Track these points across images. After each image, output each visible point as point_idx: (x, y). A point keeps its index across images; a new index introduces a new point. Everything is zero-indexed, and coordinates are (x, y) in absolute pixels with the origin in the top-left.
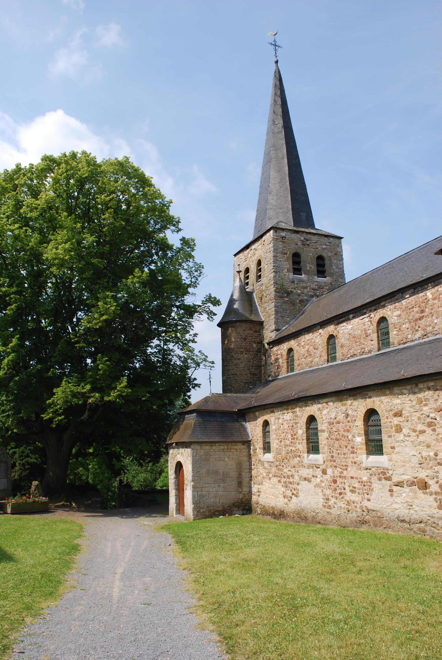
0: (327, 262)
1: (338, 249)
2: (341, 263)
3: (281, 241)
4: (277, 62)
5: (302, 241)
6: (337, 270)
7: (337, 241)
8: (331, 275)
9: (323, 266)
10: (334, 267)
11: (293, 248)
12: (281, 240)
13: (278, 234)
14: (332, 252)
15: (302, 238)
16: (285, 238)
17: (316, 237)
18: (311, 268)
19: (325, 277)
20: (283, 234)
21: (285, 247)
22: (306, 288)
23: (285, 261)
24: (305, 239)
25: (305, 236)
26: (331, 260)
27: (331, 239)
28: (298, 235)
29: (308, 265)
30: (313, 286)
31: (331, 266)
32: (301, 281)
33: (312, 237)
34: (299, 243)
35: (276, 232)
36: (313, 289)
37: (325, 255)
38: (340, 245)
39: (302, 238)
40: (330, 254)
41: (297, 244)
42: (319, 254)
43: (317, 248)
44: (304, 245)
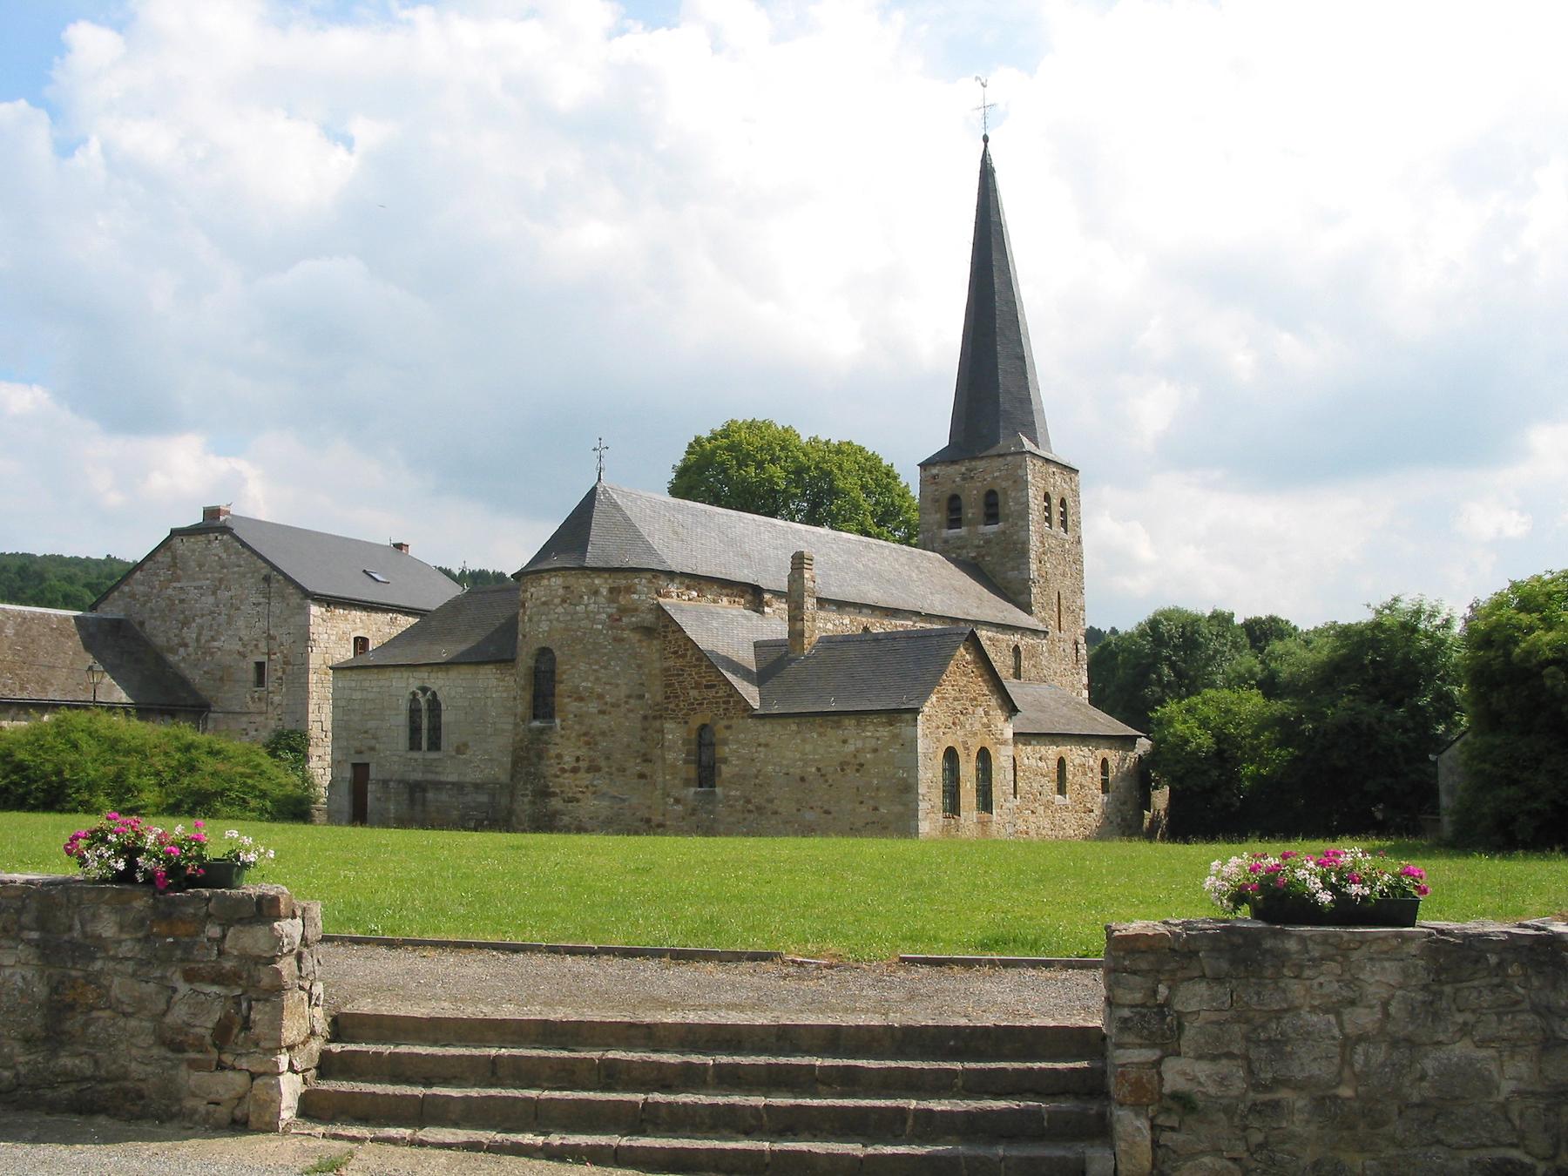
0: (1001, 498)
1: (1020, 472)
2: (1024, 493)
3: (932, 484)
4: (986, 139)
5: (963, 474)
6: (1017, 507)
7: (1019, 457)
8: (1006, 521)
9: (997, 505)
10: (1011, 504)
11: (948, 489)
12: (933, 481)
13: (928, 473)
14: (1008, 479)
15: (963, 469)
16: (938, 475)
17: (984, 462)
18: (973, 514)
19: (997, 524)
20: (935, 471)
21: (936, 490)
22: (963, 547)
23: (936, 512)
24: (967, 470)
25: (968, 464)
26: (1006, 493)
27: (1009, 458)
28: (957, 467)
29: (970, 511)
30: (976, 542)
31: (1006, 503)
32: (959, 538)
33: (978, 463)
34: (958, 479)
35: (925, 470)
36: (978, 547)
37: (997, 489)
38: (1024, 464)
39: (963, 469)
40: (1004, 484)
41: (954, 482)
42: (988, 489)
43: (985, 480)
44: (964, 479)
